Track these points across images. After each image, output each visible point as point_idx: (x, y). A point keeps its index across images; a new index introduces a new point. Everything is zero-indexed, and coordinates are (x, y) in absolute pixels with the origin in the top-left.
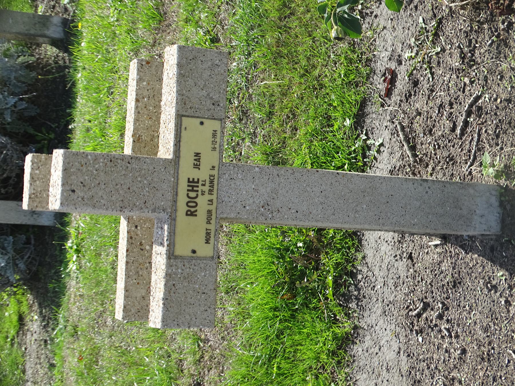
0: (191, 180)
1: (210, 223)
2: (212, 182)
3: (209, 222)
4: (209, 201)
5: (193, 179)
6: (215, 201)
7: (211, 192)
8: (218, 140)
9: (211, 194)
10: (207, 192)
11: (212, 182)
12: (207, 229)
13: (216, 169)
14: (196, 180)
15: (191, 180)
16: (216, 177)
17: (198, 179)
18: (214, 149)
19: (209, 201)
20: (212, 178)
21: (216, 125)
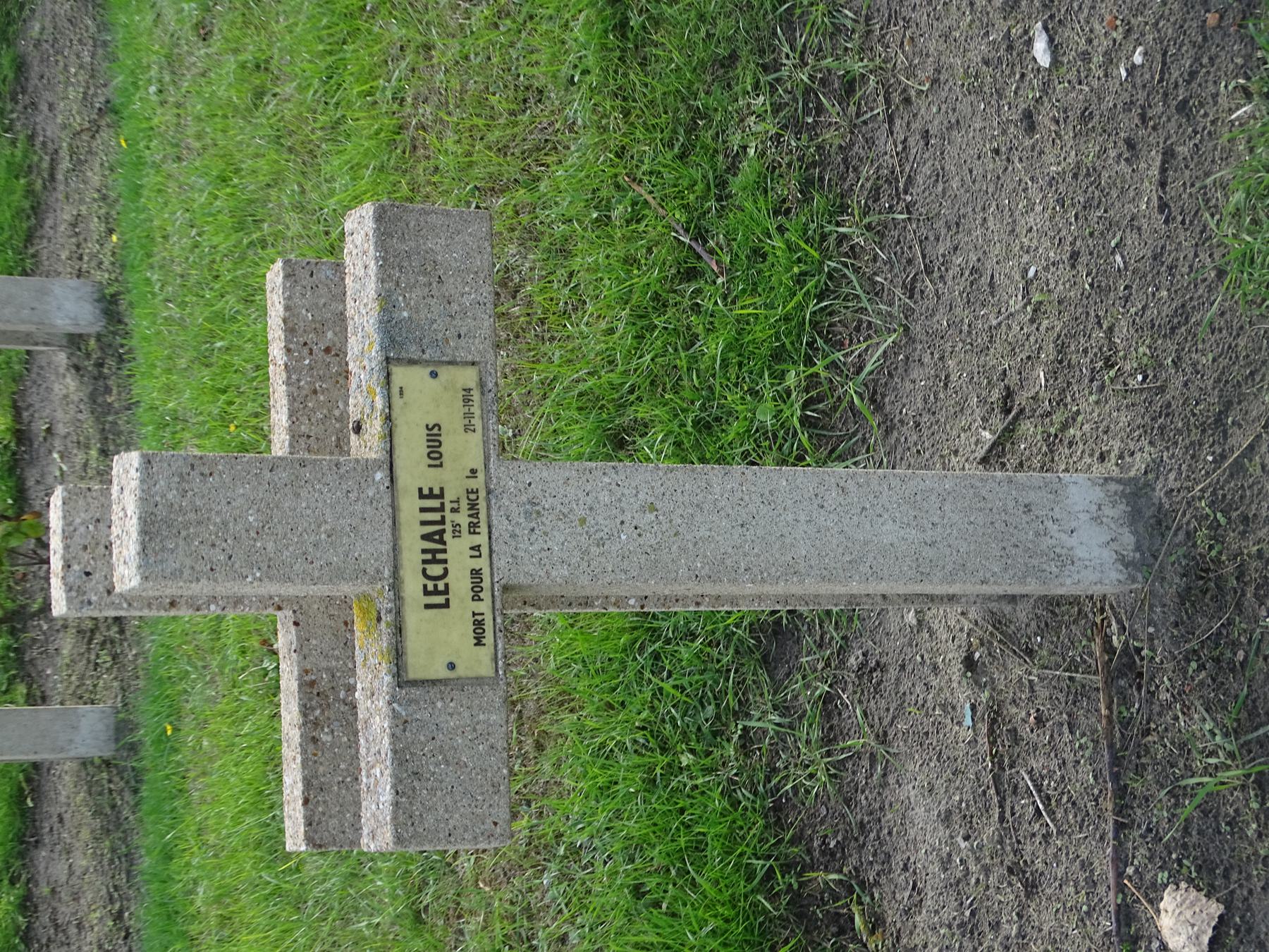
0: (426, 492)
2: (473, 506)
3: (476, 598)
4: (472, 548)
5: (431, 490)
6: (485, 551)
7: (473, 528)
8: (476, 410)
9: (475, 533)
11: (473, 506)
12: (474, 614)
13: (481, 476)
14: (437, 491)
15: (426, 492)
16: (482, 494)
17: (442, 489)
18: (468, 428)
19: (472, 548)
21: (468, 377)
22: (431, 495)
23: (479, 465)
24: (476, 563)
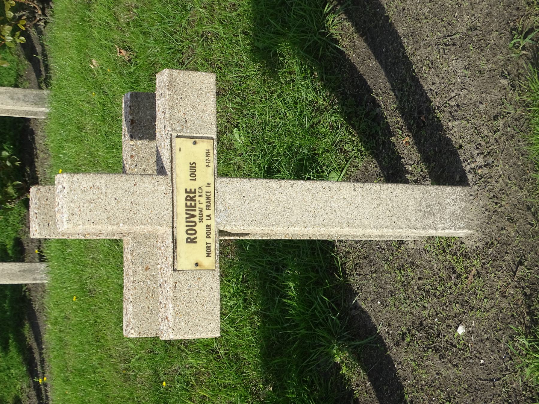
0: (188, 190)
1: (210, 238)
2: (208, 198)
3: (208, 237)
5: (191, 190)
6: (213, 217)
7: (208, 207)
9: (208, 209)
10: (204, 208)
11: (208, 198)
12: (207, 244)
13: (212, 185)
14: (193, 190)
15: (188, 190)
17: (195, 190)
20: (208, 194)
22: (191, 192)
23: (211, 180)
24: (209, 222)
